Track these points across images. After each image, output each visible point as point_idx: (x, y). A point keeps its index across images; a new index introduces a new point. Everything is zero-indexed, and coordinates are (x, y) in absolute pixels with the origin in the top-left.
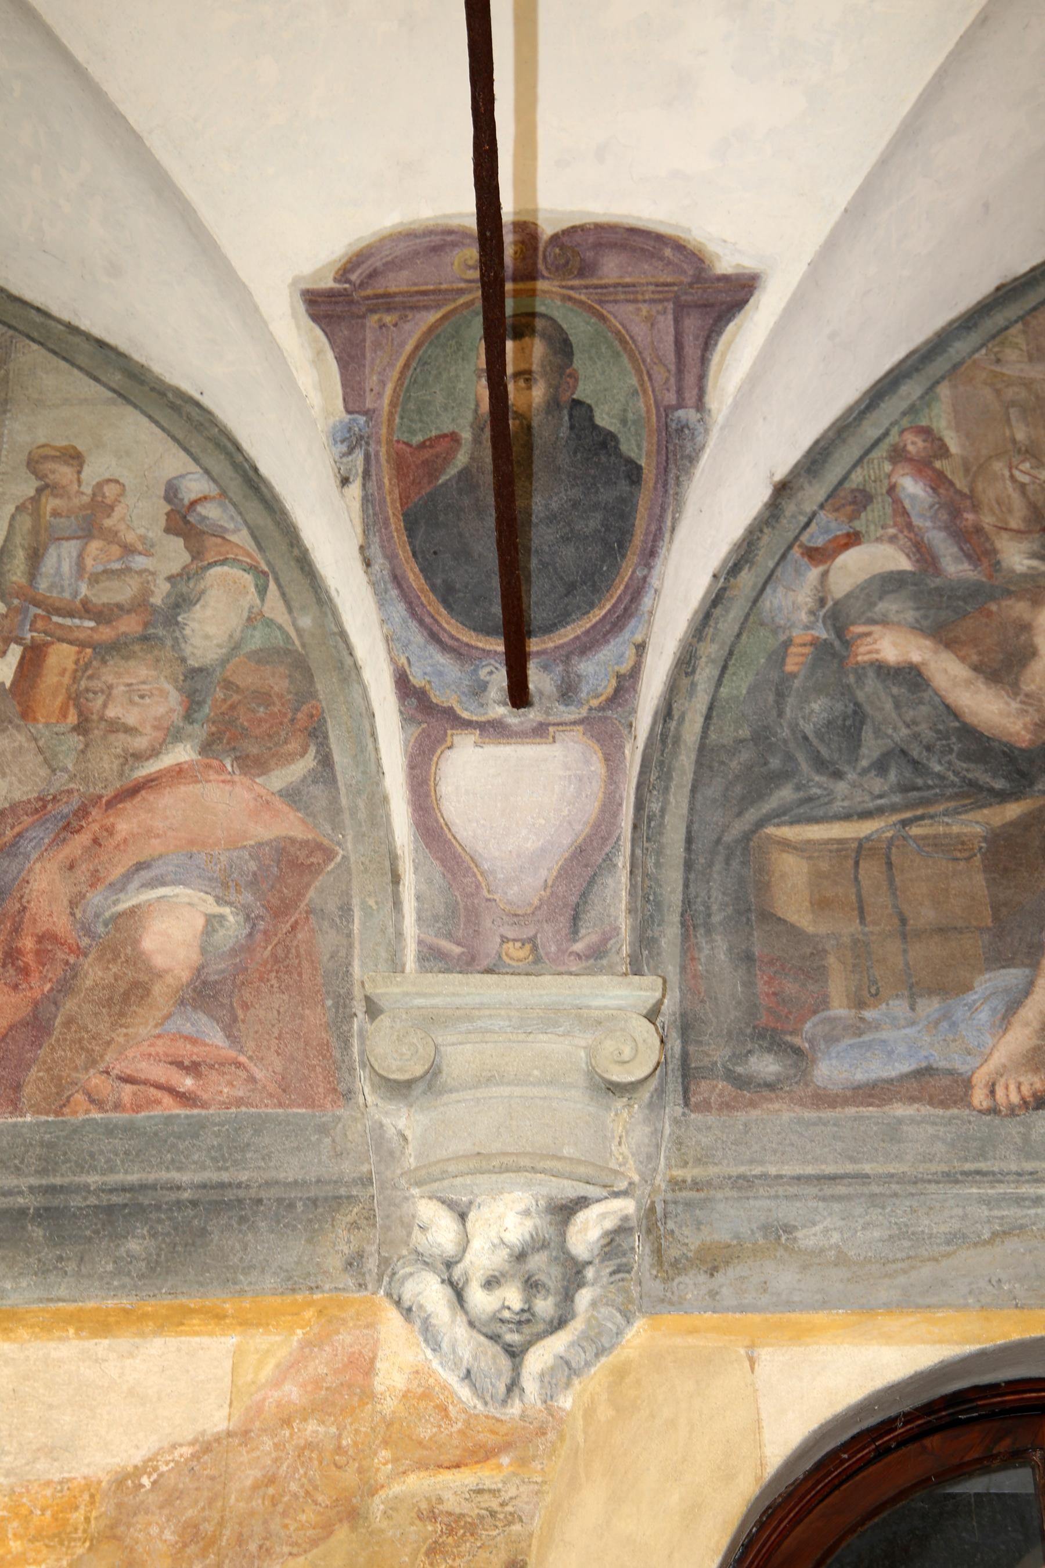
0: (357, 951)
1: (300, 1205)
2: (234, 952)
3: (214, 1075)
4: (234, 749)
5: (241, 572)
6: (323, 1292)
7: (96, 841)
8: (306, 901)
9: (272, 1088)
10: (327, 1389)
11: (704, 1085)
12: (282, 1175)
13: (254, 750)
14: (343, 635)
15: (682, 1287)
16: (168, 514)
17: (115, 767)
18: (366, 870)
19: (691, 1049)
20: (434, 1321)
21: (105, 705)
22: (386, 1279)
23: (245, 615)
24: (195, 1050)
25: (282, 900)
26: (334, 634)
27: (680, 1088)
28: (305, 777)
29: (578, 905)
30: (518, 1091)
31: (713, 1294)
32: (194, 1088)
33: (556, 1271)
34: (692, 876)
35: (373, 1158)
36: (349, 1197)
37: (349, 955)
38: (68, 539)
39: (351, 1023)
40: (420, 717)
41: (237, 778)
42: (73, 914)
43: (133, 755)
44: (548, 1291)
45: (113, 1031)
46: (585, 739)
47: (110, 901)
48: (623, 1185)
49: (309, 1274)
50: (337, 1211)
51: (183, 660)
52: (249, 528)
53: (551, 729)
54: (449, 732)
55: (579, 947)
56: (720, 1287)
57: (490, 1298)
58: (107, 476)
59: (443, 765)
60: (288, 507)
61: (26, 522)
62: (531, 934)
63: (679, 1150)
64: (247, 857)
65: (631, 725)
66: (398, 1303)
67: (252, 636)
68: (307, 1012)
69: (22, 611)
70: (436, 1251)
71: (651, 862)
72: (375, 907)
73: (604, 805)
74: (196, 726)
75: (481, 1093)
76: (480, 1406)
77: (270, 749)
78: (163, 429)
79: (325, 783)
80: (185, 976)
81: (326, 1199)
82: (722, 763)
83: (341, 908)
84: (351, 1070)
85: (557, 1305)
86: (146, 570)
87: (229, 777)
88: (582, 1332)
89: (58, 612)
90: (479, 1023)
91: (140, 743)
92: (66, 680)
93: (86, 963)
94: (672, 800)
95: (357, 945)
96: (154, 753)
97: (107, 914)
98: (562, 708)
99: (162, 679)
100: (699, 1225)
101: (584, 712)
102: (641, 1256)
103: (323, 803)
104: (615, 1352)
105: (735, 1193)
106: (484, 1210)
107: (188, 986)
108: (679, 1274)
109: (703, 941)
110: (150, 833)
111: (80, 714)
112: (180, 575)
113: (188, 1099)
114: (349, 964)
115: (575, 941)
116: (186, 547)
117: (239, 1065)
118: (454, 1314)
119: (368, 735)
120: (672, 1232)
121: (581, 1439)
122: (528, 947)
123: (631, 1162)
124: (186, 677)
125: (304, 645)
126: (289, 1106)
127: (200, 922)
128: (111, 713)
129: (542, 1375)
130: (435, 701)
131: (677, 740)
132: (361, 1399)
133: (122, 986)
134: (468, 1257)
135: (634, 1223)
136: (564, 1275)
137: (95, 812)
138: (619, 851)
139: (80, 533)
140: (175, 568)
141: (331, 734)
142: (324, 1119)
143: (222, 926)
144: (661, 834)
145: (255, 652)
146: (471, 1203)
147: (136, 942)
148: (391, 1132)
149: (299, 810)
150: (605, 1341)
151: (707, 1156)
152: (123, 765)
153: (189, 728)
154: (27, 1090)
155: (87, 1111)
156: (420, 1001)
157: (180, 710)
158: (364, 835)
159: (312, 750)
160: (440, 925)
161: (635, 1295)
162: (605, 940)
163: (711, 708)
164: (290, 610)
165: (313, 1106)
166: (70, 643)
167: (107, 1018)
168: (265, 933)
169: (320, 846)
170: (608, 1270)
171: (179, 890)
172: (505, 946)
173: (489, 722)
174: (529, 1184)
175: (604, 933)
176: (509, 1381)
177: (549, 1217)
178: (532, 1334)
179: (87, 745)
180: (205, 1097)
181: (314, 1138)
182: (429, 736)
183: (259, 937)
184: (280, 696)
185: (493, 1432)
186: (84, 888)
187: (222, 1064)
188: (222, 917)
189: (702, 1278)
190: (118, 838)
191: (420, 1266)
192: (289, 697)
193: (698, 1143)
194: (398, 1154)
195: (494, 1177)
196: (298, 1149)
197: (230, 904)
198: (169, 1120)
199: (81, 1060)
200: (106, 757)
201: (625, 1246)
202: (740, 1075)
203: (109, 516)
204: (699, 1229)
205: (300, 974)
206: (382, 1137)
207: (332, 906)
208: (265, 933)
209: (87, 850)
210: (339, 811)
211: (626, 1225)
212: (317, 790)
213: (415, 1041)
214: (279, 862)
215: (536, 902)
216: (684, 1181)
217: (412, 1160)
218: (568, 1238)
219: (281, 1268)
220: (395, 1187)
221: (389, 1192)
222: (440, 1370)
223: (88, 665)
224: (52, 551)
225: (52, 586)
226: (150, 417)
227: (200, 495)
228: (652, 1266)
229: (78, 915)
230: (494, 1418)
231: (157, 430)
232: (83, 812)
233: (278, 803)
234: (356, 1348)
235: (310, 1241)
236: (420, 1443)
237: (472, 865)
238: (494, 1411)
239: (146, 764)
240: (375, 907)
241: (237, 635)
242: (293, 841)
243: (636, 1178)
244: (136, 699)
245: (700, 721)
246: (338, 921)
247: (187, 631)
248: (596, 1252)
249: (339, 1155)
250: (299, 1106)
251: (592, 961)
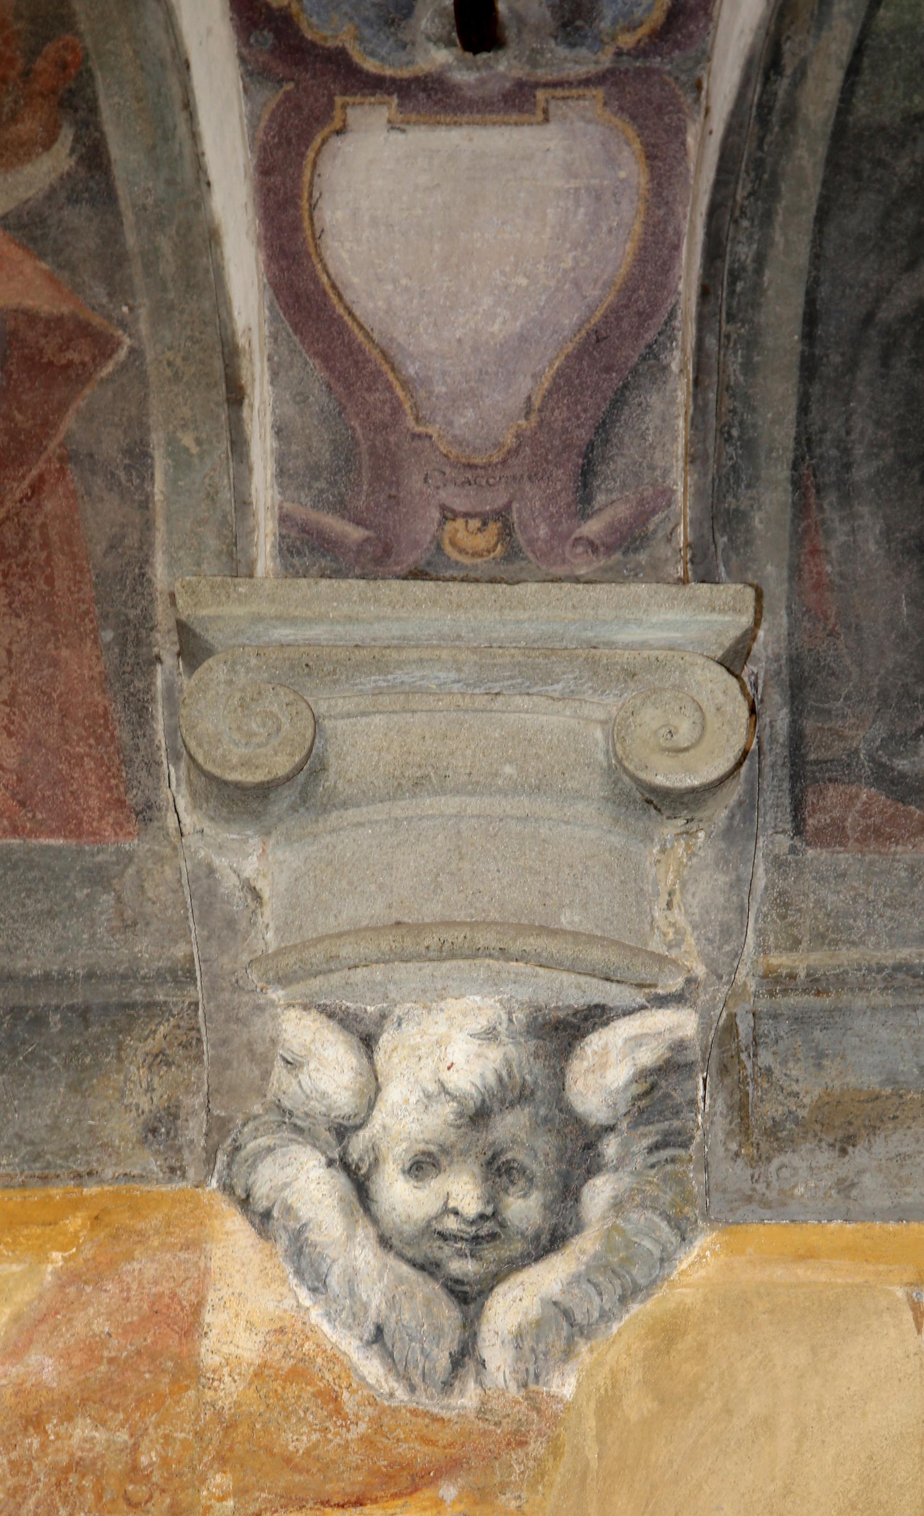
0: (160, 536)
1: (55, 1019)
6: (101, 1182)
8: (60, 437)
10: (111, 1361)
11: (832, 793)
12: (21, 964)
15: (785, 1173)
18: (177, 378)
19: (809, 725)
20: (313, 1236)
22: (222, 1158)
27: (787, 801)
29: (591, 446)
30: (473, 804)
31: (845, 1187)
33: (545, 1144)
34: (816, 389)
35: (196, 931)
36: (150, 1006)
37: (145, 545)
39: (151, 674)
40: (280, 69)
44: (531, 1180)
46: (608, 113)
48: (675, 984)
49: (74, 1149)
50: (128, 1031)
53: (541, 94)
54: (339, 100)
55: (592, 528)
56: (860, 1173)
57: (420, 1194)
59: (325, 168)
62: (500, 502)
63: (783, 917)
65: (698, 86)
66: (245, 1203)
68: (65, 653)
70: (318, 1107)
71: (734, 364)
72: (195, 450)
73: (644, 248)
75: (401, 808)
76: (401, 1394)
81: (105, 1009)
82: (879, 163)
83: (128, 452)
84: (152, 765)
85: (547, 1207)
88: (595, 1257)
90: (399, 676)
94: (778, 237)
95: (160, 522)
98: (562, 51)
100: (819, 1058)
101: (606, 60)
102: (709, 1118)
104: (658, 1295)
105: (890, 1000)
106: (409, 1029)
108: (781, 1150)
109: (833, 516)
114: (146, 561)
115: (585, 516)
118: (351, 1226)
119: (178, 106)
120: (769, 1070)
121: (592, 1454)
122: (494, 528)
123: (691, 940)
126: (32, 833)
129: (519, 1337)
130: (309, 36)
131: (790, 117)
132: (175, 1381)
134: (379, 1117)
135: (695, 1054)
136: (562, 1151)
138: (672, 339)
142: (99, 858)
144: (755, 305)
146: (383, 1016)
148: (230, 882)
149: (41, 256)
150: (638, 1273)
151: (836, 929)
156: (283, 633)
158: (171, 308)
159: (67, 135)
160: (321, 484)
161: (697, 1188)
162: (643, 515)
163: (858, 51)
165: (78, 832)
169: (85, 330)
170: (646, 1142)
172: (449, 526)
173: (416, 79)
174: (494, 982)
175: (641, 501)
176: (455, 1348)
177: (532, 1044)
178: (499, 1261)
181: (81, 894)
182: (298, 108)
185: (425, 1440)
189: (825, 1157)
191: (287, 1134)
192: (19, 25)
193: (820, 903)
194: (243, 925)
195: (428, 968)
196: (51, 914)
201: (678, 1097)
202: (903, 775)
204: (819, 1066)
205: (50, 580)
206: (211, 891)
210: (121, 260)
211: (681, 1059)
213: (275, 708)
215: (509, 440)
216: (792, 976)
217: (270, 936)
218: (569, 1082)
219: (20, 1137)
220: (237, 987)
221: (226, 995)
222: (326, 1327)
228: (729, 1134)
230: (426, 1414)
234: (165, 1287)
235: (75, 1087)
236: (288, 1460)
237: (385, 368)
238: (426, 1401)
240: (195, 450)
242: (31, 317)
243: (700, 971)
245: (835, 78)
246: (122, 476)
248: (622, 1110)
249: (129, 926)
250: (52, 833)
251: (618, 556)
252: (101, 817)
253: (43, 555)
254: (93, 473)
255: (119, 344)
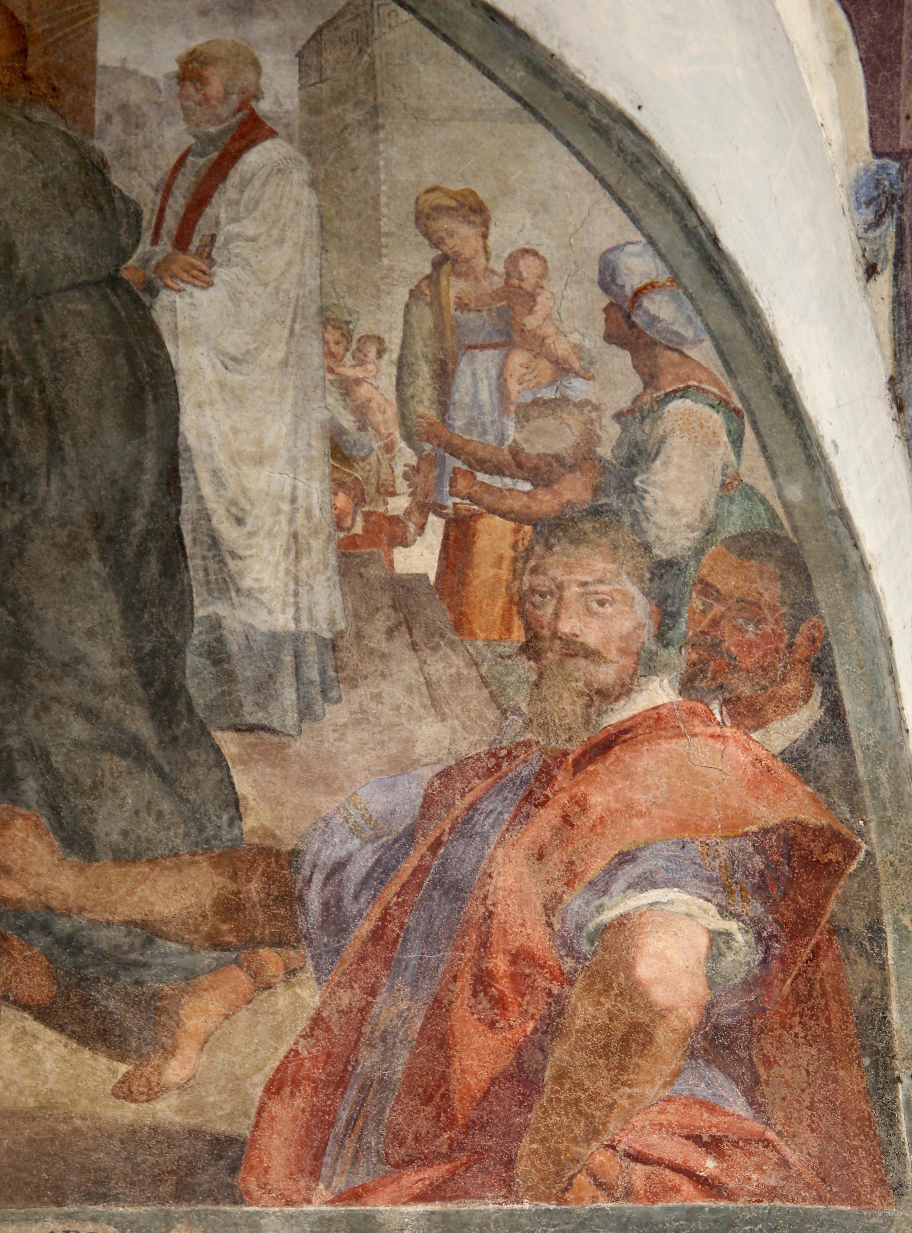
0: (893, 990)
2: (748, 985)
3: (738, 1156)
4: (721, 687)
5: (708, 410)
7: (566, 819)
8: (827, 916)
9: (809, 1176)
13: (746, 690)
14: (843, 514)
16: (605, 310)
17: (579, 711)
18: (896, 874)
21: (557, 615)
23: (719, 478)
24: (715, 1121)
25: (799, 912)
26: (832, 513)
28: (811, 733)
32: (716, 1172)
37: (885, 995)
38: (482, 347)
39: (894, 1090)
41: (728, 732)
42: (550, 925)
43: (598, 692)
45: (615, 1090)
47: (592, 907)
51: (647, 548)
52: (713, 338)
58: (521, 244)
60: (763, 304)
61: (425, 318)
64: (751, 850)
67: (730, 513)
68: (842, 1073)
69: (435, 462)
74: (672, 650)
77: (765, 688)
78: (589, 167)
79: (835, 741)
80: (693, 1017)
86: (587, 402)
87: (718, 730)
89: (482, 464)
91: (606, 674)
92: (505, 573)
93: (574, 993)
96: (624, 690)
97: (591, 926)
99: (624, 577)
103: (835, 773)
107: (697, 1032)
110: (630, 809)
111: (528, 627)
112: (631, 411)
113: (712, 1187)
114: (886, 1008)
116: (635, 367)
117: (767, 1143)
119: (885, 672)
124: (653, 574)
125: (795, 529)
126: (831, 1201)
127: (703, 941)
128: (566, 627)
133: (619, 1029)
137: (562, 777)
139: (497, 339)
140: (625, 403)
141: (839, 669)
142: (873, 1221)
143: (729, 948)
145: (735, 538)
147: (629, 968)
149: (807, 782)
152: (589, 706)
153: (663, 653)
154: (521, 1167)
155: (594, 1199)
157: (650, 626)
158: (890, 823)
159: (817, 691)
164: (774, 475)
165: (858, 1202)
166: (503, 515)
167: (605, 1073)
168: (782, 959)
169: (837, 837)
171: (673, 894)
179: (541, 675)
180: (731, 1185)
183: (775, 964)
184: (773, 609)
186: (559, 887)
187: (747, 1141)
188: (728, 934)
190: (594, 814)
197: (736, 916)
198: (692, 1214)
199: (579, 1130)
200: (566, 695)
203: (531, 311)
205: (828, 1020)
207: (859, 925)
208: (782, 959)
209: (557, 831)
210: (856, 786)
212: (826, 753)
214: (789, 858)
223: (529, 552)
224: (464, 366)
225: (470, 424)
226: (568, 144)
227: (646, 281)
229: (557, 927)
231: (580, 168)
232: (545, 776)
233: (781, 770)
239: (616, 706)
241: (711, 511)
244: (595, 605)
247: (648, 503)
250: (843, 1202)
252: (872, 1192)
253: (823, 1002)
254: (850, 943)
255: (860, 848)
